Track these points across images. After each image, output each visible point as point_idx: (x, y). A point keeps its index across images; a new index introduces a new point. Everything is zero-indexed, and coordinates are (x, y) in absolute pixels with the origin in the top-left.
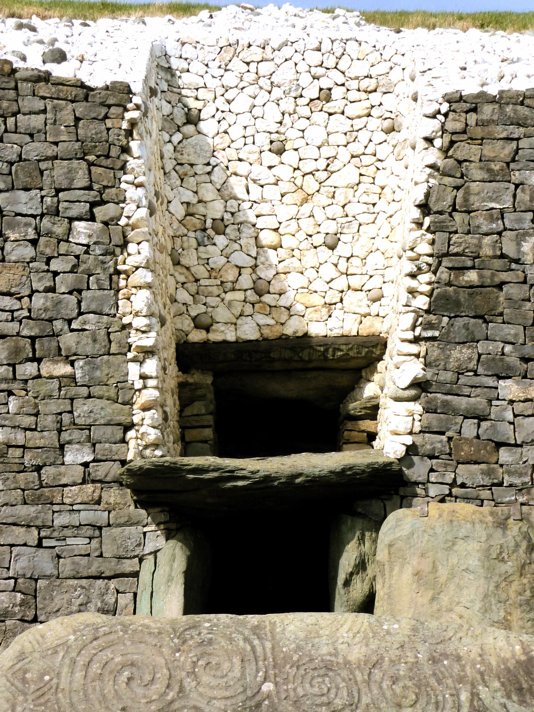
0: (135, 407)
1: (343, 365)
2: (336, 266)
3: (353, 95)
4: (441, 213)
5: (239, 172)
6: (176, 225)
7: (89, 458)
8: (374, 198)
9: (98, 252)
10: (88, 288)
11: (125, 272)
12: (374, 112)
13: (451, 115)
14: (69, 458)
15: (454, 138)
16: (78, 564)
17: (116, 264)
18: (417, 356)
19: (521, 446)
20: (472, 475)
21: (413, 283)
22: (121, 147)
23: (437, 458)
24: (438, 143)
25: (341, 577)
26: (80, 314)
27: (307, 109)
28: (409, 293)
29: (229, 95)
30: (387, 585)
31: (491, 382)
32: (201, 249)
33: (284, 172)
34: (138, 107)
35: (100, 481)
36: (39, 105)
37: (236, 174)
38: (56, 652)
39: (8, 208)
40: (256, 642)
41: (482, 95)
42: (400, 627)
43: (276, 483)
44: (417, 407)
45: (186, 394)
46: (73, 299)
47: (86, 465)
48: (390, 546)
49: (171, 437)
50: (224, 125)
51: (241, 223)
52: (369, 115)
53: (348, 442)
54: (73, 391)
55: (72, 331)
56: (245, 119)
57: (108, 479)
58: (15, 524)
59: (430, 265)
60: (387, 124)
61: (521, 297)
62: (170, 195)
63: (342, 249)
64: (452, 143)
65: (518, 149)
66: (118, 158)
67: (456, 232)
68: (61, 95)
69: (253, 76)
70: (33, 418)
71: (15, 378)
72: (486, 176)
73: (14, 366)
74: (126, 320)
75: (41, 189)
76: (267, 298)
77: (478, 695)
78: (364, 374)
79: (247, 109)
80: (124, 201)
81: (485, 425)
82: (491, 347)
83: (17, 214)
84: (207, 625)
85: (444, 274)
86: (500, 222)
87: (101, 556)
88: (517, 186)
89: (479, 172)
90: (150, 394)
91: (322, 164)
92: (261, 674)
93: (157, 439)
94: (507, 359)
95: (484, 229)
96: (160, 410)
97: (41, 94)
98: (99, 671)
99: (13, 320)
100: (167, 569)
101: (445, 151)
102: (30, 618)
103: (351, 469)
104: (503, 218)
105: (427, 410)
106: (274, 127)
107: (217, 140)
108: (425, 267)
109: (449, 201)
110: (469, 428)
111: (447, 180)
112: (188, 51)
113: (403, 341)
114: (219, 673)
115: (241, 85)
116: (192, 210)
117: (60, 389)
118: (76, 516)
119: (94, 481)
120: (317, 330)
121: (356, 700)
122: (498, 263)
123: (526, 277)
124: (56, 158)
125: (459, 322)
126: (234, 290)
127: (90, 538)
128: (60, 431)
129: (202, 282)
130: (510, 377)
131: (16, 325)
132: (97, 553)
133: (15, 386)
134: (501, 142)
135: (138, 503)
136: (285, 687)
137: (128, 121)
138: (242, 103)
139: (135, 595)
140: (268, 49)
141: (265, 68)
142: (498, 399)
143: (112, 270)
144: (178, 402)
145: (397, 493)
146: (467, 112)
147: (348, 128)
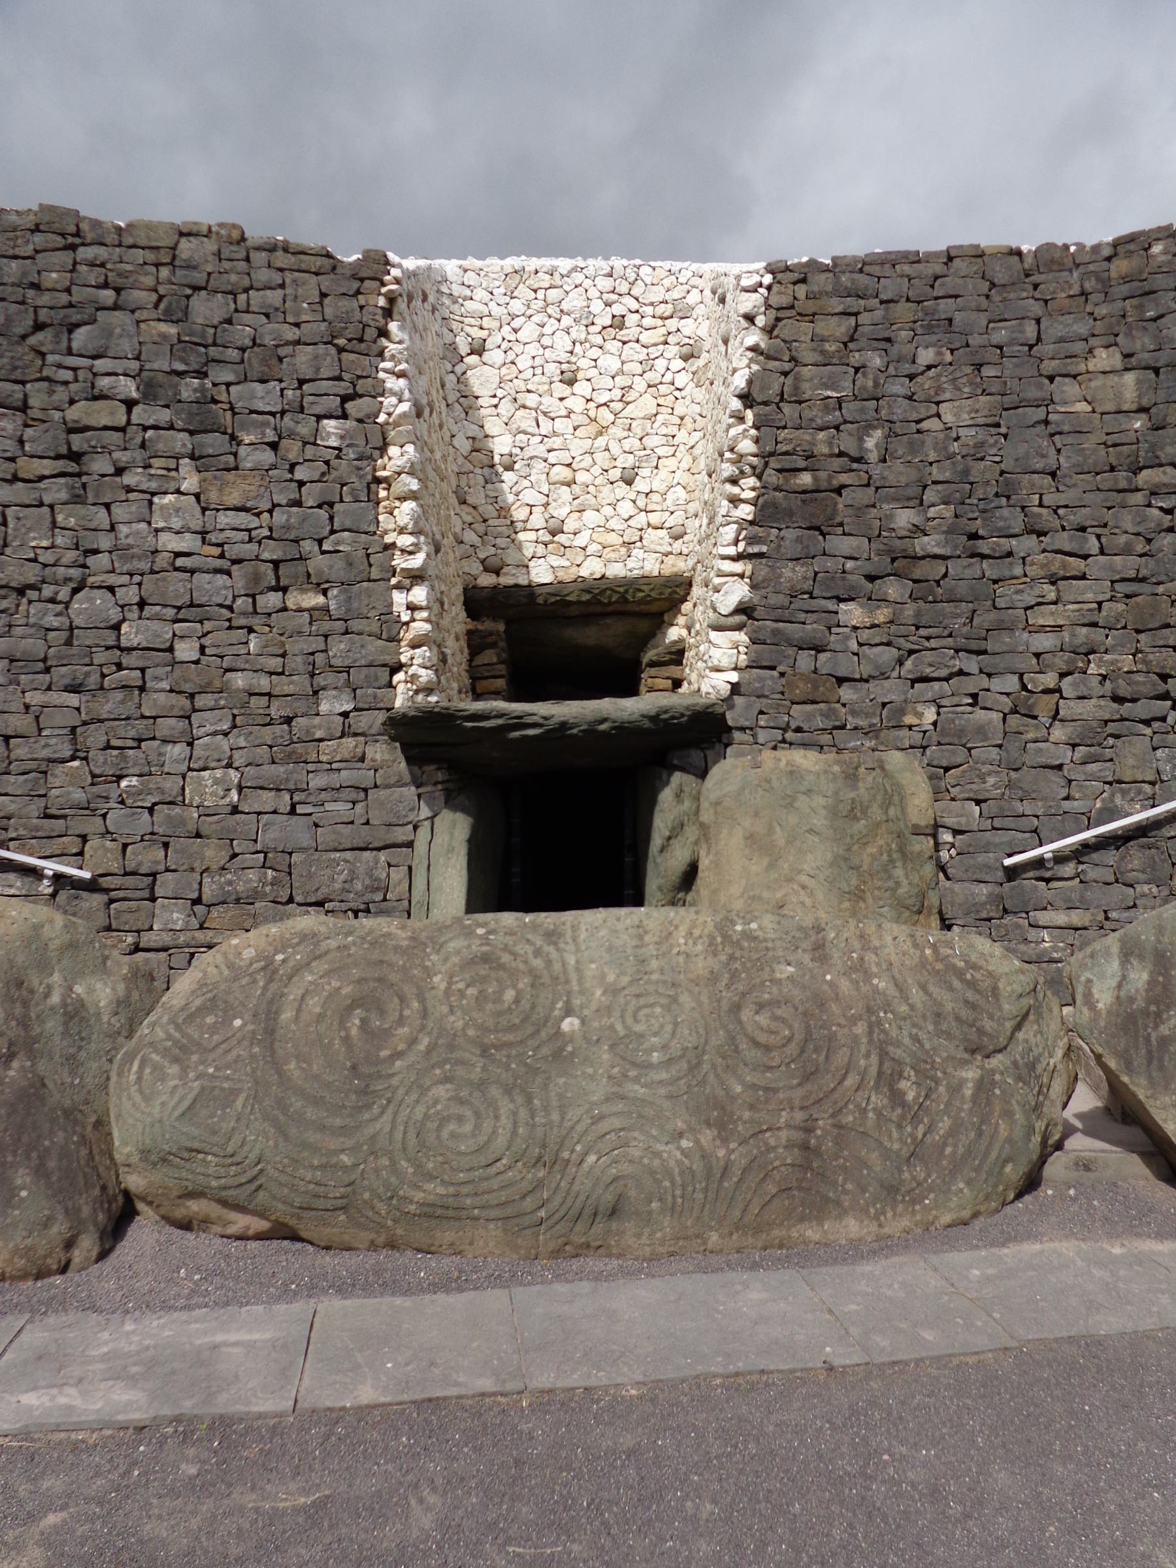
0: (403, 643)
1: (644, 608)
2: (634, 502)
3: (648, 322)
4: (765, 403)
5: (528, 404)
6: (461, 460)
7: (347, 707)
8: (673, 430)
9: (352, 456)
10: (342, 501)
11: (386, 480)
12: (671, 339)
13: (775, 288)
14: (324, 707)
15: (781, 314)
16: (339, 833)
17: (375, 470)
18: (742, 576)
19: (867, 681)
20: (810, 717)
21: (736, 490)
22: (378, 329)
23: (766, 697)
24: (761, 321)
25: (656, 841)
26: (333, 532)
27: (599, 337)
28: (731, 501)
29: (516, 323)
30: (713, 851)
31: (831, 605)
32: (489, 486)
33: (577, 404)
34: (397, 281)
35: (363, 734)
36: (277, 278)
37: (524, 407)
38: (255, 981)
39: (240, 404)
40: (554, 955)
41: (812, 263)
42: (760, 928)
43: (575, 731)
44: (742, 637)
45: (476, 643)
46: (323, 514)
47: (345, 715)
48: (718, 803)
49: (455, 685)
50: (511, 356)
51: (531, 458)
52: (666, 343)
53: (651, 690)
54: (326, 626)
55: (323, 553)
56: (533, 349)
57: (373, 731)
58: (262, 788)
59: (753, 468)
60: (685, 350)
61: (866, 502)
62: (455, 429)
63: (641, 485)
64: (778, 319)
65: (857, 326)
66: (375, 342)
67: (785, 427)
68: (303, 266)
69: (541, 304)
70: (280, 660)
71: (255, 612)
72: (818, 358)
73: (253, 596)
74: (389, 539)
75: (281, 381)
76: (560, 538)
77: (879, 1023)
78: (666, 617)
79: (535, 336)
80: (382, 395)
81: (823, 657)
82: (829, 564)
83: (252, 412)
84: (480, 931)
85: (771, 477)
86: (837, 413)
87: (367, 823)
88: (856, 372)
89: (811, 354)
90: (420, 627)
91: (617, 394)
92: (560, 1005)
93: (429, 681)
94: (849, 577)
95: (819, 421)
96: (435, 649)
97: (279, 264)
98: (318, 1010)
99: (250, 540)
100: (447, 838)
101: (769, 331)
102: (284, 900)
103: (666, 712)
104: (840, 409)
105: (754, 642)
106: (564, 357)
107: (504, 371)
108: (747, 469)
109: (776, 388)
110: (805, 661)
111: (773, 364)
112: (470, 279)
113: (724, 558)
114: (498, 1007)
115: (529, 312)
116: (477, 445)
117: (310, 623)
118: (335, 775)
119: (355, 735)
120: (616, 570)
121: (702, 1040)
122: (837, 463)
123: (870, 478)
124: (298, 342)
125: (790, 534)
126: (525, 530)
127: (354, 803)
128: (312, 675)
129: (490, 522)
130: (853, 599)
131: (255, 546)
132: (363, 820)
133: (255, 622)
134: (836, 318)
135: (409, 760)
136: (596, 1024)
137: (385, 295)
138: (528, 331)
139: (410, 868)
140: (557, 276)
141: (553, 294)
142: (839, 626)
143: (370, 477)
144: (466, 651)
145: (720, 741)
146: (795, 283)
147: (643, 357)
